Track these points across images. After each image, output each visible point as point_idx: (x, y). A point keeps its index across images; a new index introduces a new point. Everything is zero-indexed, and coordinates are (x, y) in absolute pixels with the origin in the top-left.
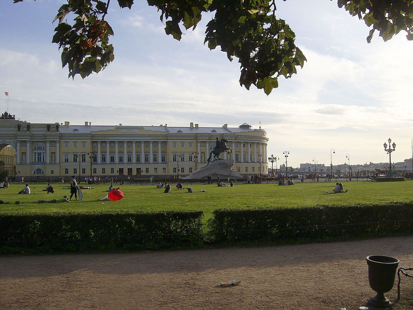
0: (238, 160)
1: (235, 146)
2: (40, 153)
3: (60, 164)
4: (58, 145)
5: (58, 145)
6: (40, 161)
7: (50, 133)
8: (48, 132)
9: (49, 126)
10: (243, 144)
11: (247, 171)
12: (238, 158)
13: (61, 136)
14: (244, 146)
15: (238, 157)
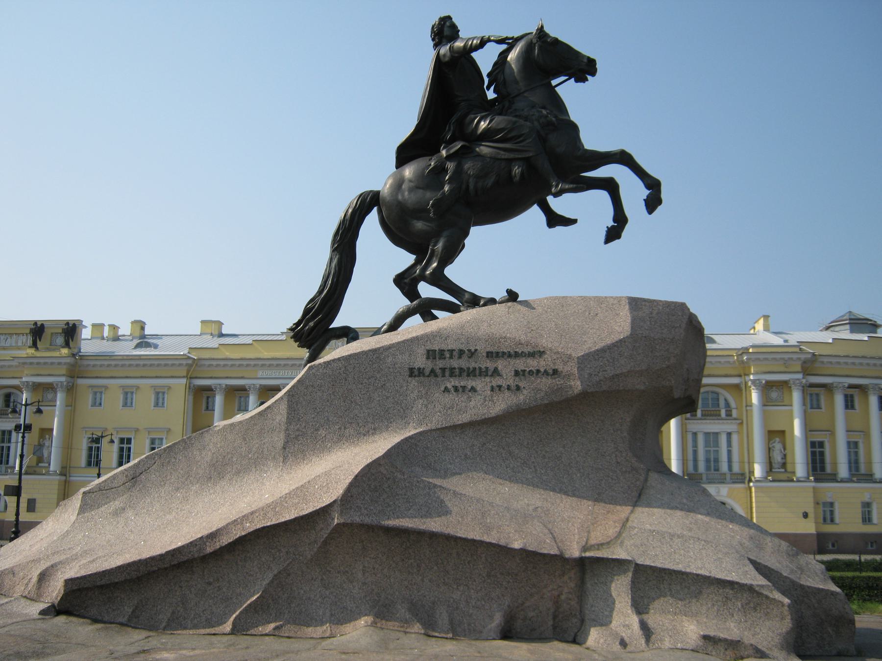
0: (823, 469)
1: (809, 406)
2: (10, 432)
3: (65, 475)
4: (60, 398)
5: (60, 398)
6: (7, 462)
7: (38, 354)
8: (31, 351)
9: (38, 330)
10: (846, 396)
11: (867, 519)
12: (823, 461)
13: (79, 368)
14: (849, 404)
15: (822, 454)
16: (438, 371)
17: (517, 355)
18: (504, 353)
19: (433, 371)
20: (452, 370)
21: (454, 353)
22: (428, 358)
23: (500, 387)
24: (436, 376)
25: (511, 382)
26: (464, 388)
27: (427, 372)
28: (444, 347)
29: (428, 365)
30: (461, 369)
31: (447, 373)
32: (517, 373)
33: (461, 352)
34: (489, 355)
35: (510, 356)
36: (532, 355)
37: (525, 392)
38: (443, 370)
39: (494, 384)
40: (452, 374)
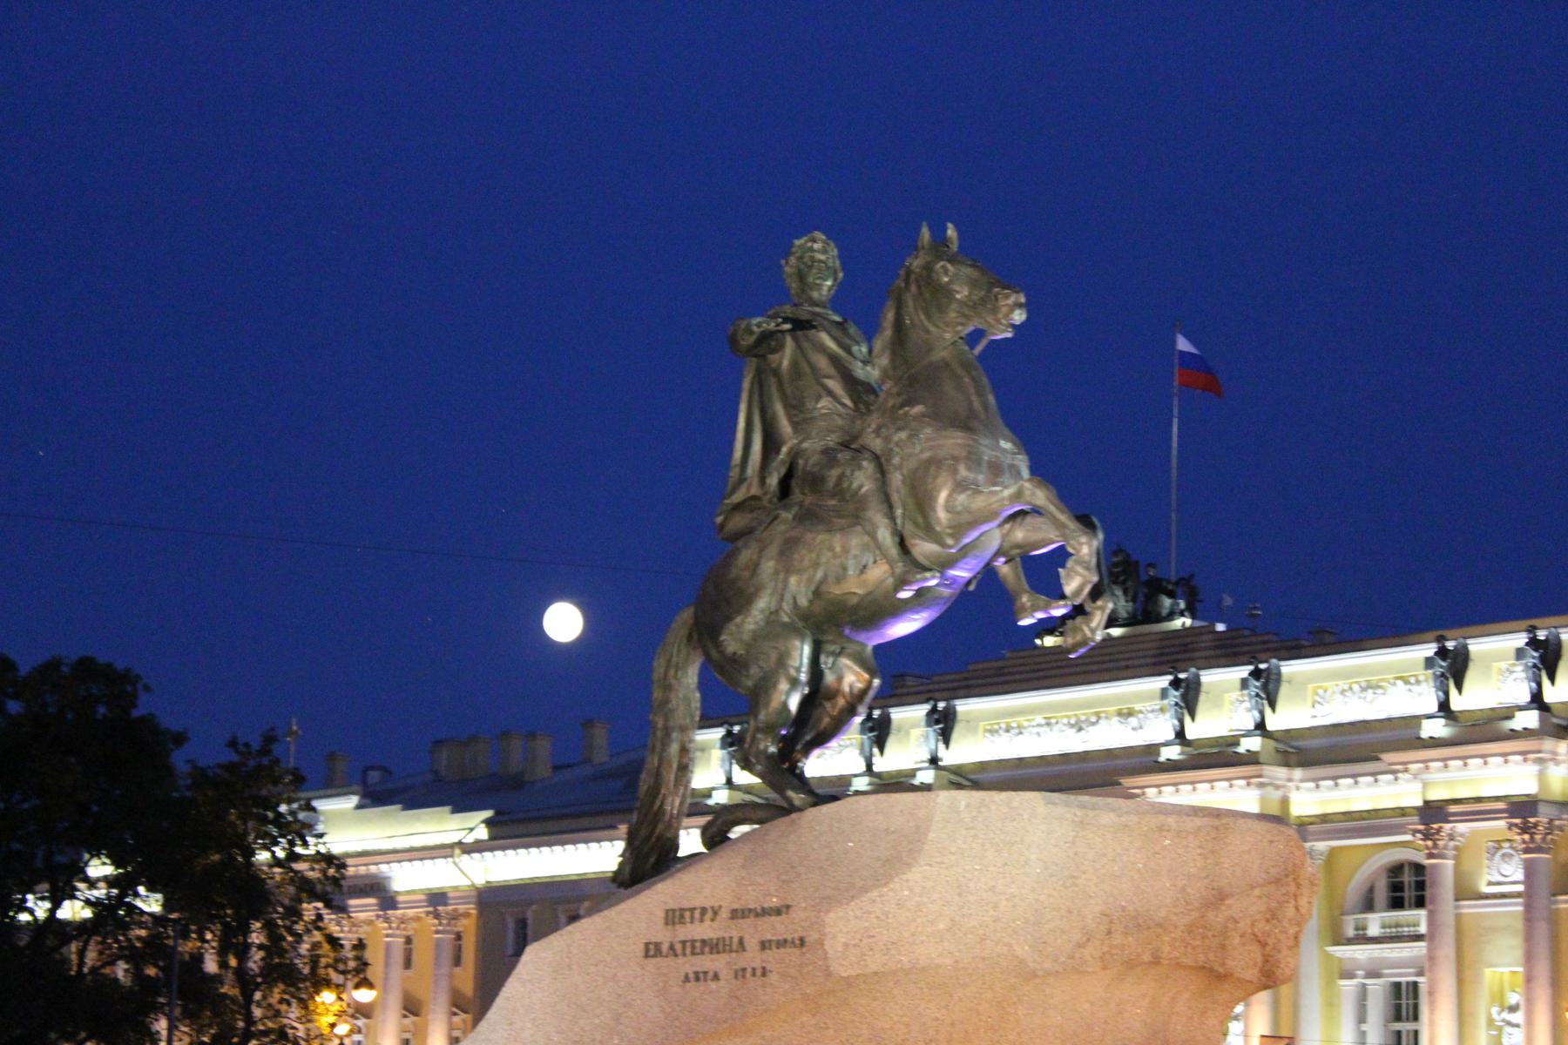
16: (678, 947)
17: (765, 912)
18: (750, 910)
19: (672, 947)
20: (693, 941)
21: (697, 914)
22: (667, 924)
23: (744, 970)
24: (676, 955)
25: (757, 964)
26: (705, 973)
27: (665, 948)
28: (686, 905)
29: (664, 936)
30: (703, 942)
31: (688, 951)
32: (764, 945)
33: (704, 911)
34: (736, 914)
35: (757, 915)
36: (778, 911)
37: (774, 978)
38: (684, 943)
39: (742, 964)
40: (693, 954)
